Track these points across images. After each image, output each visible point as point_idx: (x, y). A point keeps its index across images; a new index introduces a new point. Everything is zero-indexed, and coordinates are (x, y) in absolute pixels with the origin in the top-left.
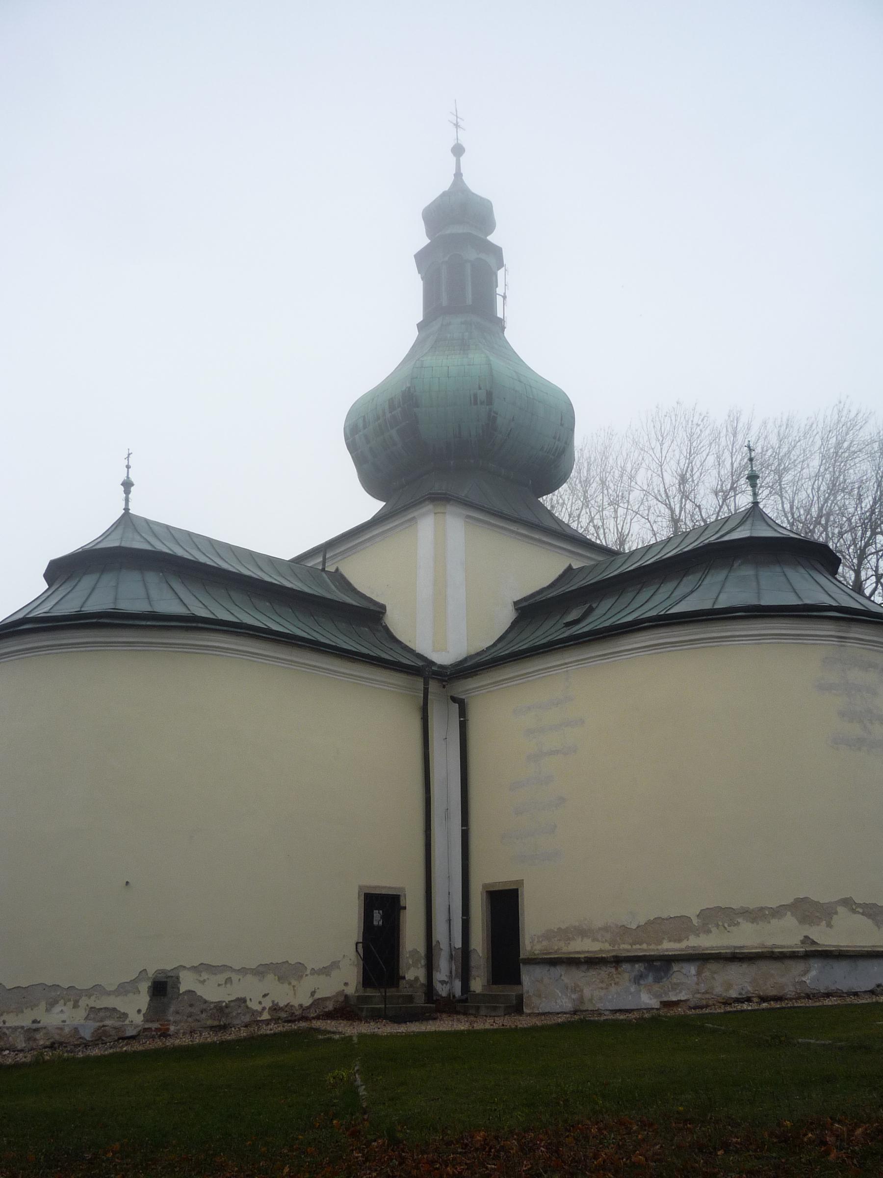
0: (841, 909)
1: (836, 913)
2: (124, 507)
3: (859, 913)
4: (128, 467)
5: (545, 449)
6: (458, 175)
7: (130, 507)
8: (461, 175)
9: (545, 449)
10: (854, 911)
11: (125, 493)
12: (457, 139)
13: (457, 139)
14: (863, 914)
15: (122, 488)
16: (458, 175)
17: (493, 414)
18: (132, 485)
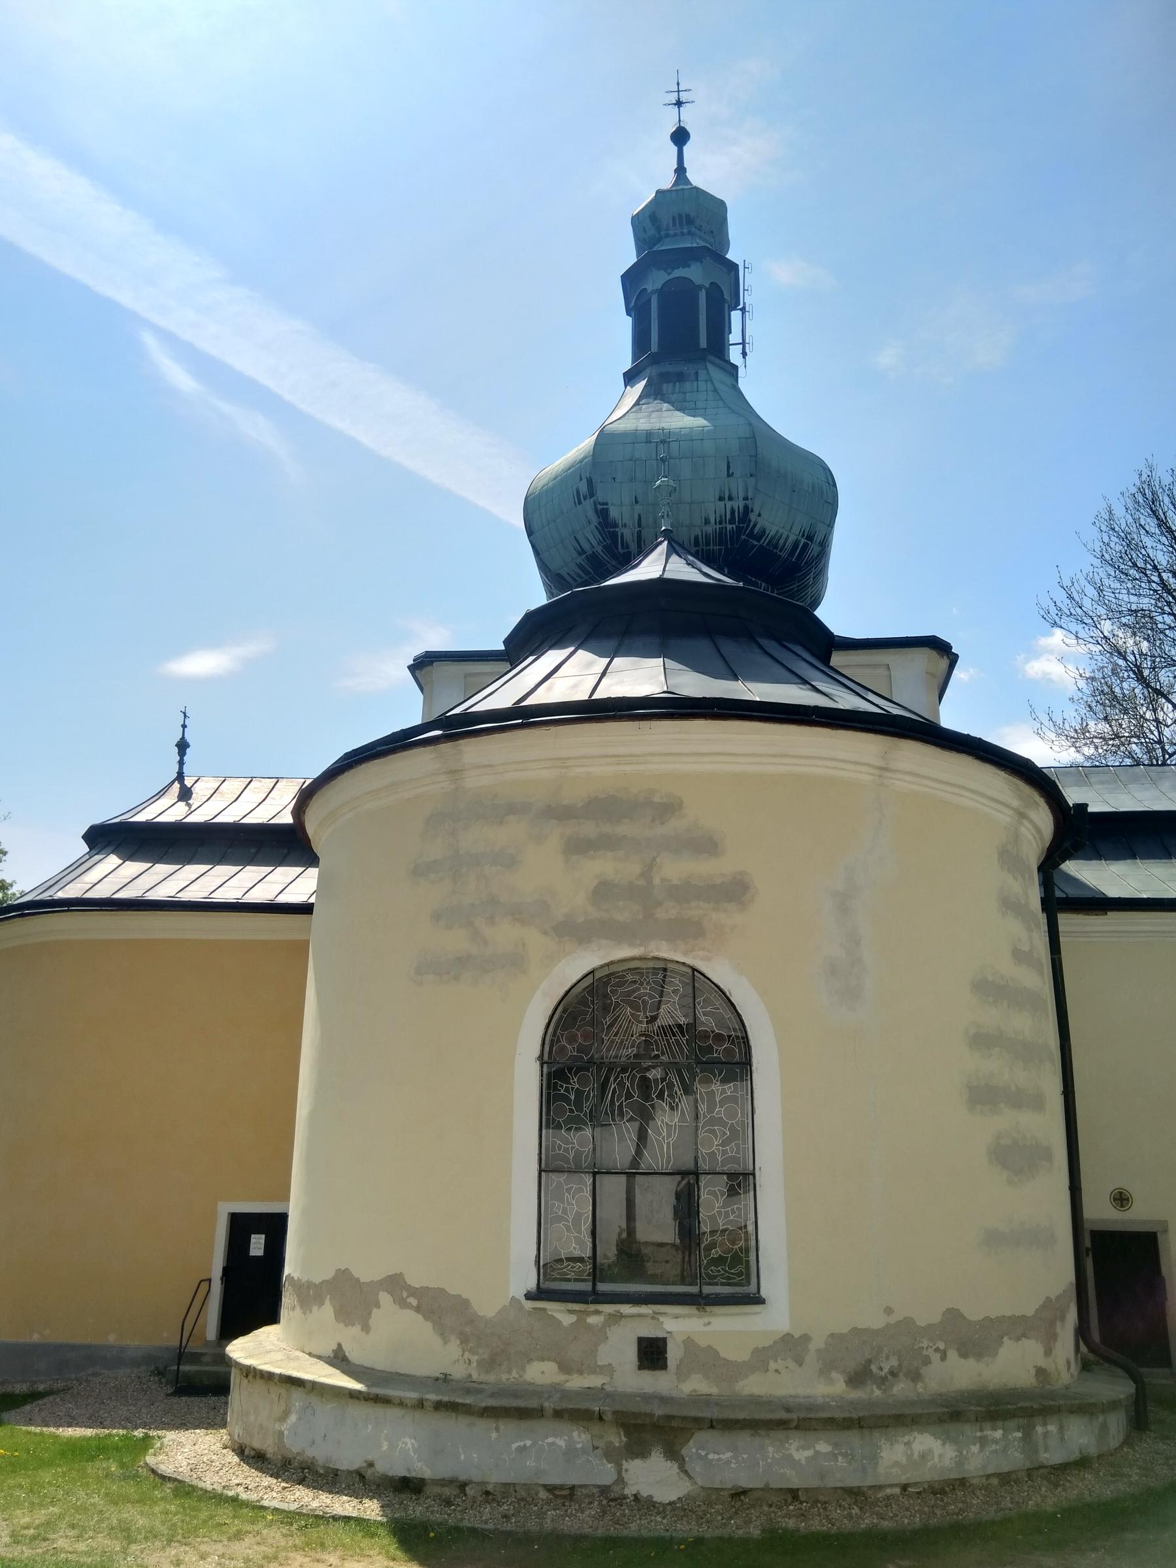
0: (384, 1298)
1: (378, 1306)
2: (177, 771)
3: (410, 1306)
4: (184, 726)
5: (713, 521)
6: (681, 170)
7: (184, 771)
8: (684, 170)
9: (713, 521)
10: (403, 1304)
11: (179, 755)
12: (680, 121)
13: (680, 121)
14: (418, 1309)
15: (176, 750)
16: (681, 170)
17: (600, 507)
18: (189, 746)
